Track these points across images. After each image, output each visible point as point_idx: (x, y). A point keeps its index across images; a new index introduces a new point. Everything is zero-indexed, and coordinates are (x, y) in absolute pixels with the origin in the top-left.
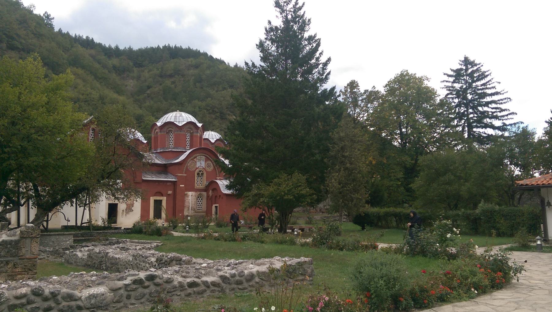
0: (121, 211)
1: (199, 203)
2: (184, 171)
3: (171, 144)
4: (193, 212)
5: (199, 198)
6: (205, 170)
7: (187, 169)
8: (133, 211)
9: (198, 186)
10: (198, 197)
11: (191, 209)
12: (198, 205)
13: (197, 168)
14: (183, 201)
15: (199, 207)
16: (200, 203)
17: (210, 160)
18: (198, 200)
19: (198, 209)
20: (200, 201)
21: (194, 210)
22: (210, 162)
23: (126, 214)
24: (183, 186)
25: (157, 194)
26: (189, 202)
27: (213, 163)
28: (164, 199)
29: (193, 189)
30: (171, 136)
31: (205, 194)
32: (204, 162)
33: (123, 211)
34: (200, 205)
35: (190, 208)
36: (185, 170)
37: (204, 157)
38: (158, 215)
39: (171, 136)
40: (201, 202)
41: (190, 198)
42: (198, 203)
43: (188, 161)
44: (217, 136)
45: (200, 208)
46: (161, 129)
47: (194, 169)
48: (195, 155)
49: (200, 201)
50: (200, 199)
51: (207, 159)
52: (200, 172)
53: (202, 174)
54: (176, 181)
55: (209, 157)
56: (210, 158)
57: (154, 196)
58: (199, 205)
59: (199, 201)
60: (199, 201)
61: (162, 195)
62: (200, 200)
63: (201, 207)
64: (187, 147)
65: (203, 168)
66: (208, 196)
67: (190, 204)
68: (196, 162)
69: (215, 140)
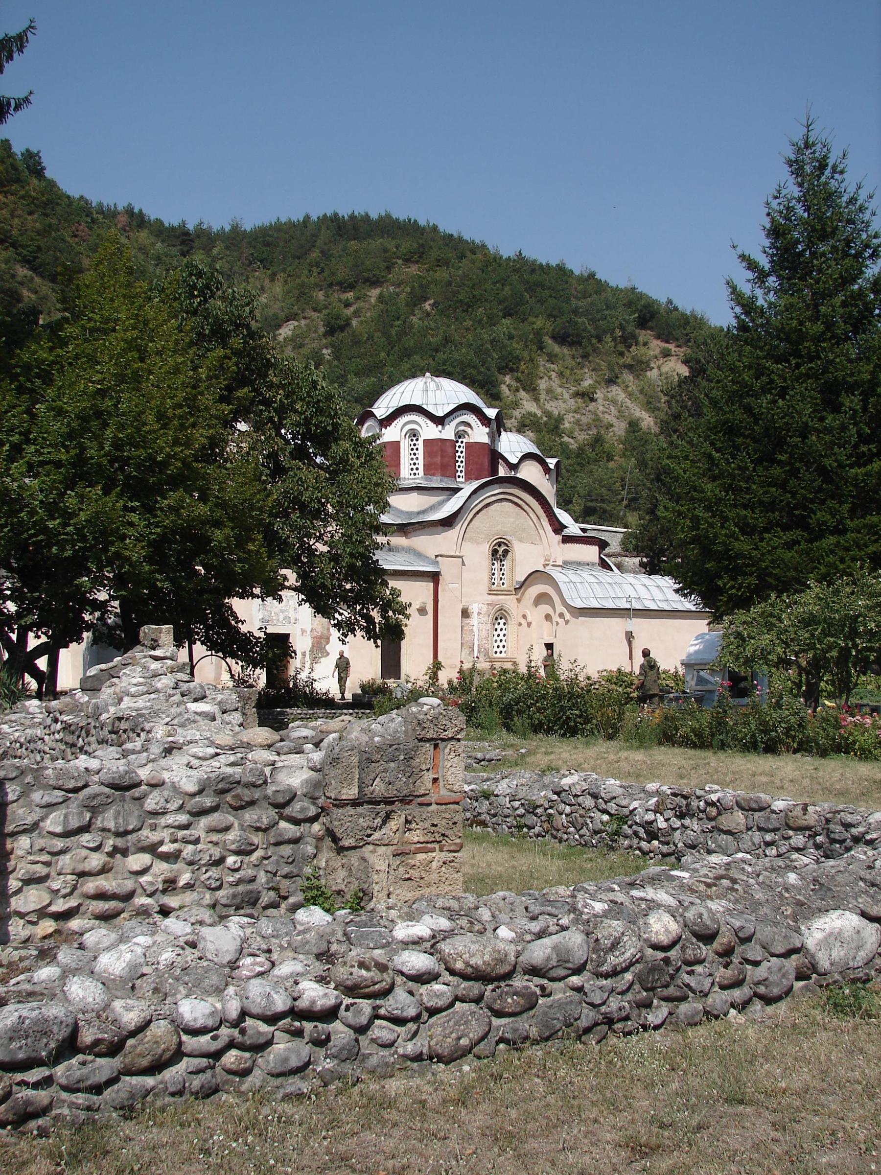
1: (499, 635)
10: (496, 619)
11: (479, 652)
12: (496, 641)
15: (498, 647)
16: (502, 633)
18: (496, 626)
19: (496, 652)
20: (501, 630)
33: (304, 654)
34: (501, 641)
44: (522, 444)
45: (501, 648)
49: (501, 630)
50: (502, 621)
52: (500, 546)
58: (499, 639)
59: (499, 628)
62: (502, 625)
63: (504, 647)
64: (459, 477)
69: (520, 455)
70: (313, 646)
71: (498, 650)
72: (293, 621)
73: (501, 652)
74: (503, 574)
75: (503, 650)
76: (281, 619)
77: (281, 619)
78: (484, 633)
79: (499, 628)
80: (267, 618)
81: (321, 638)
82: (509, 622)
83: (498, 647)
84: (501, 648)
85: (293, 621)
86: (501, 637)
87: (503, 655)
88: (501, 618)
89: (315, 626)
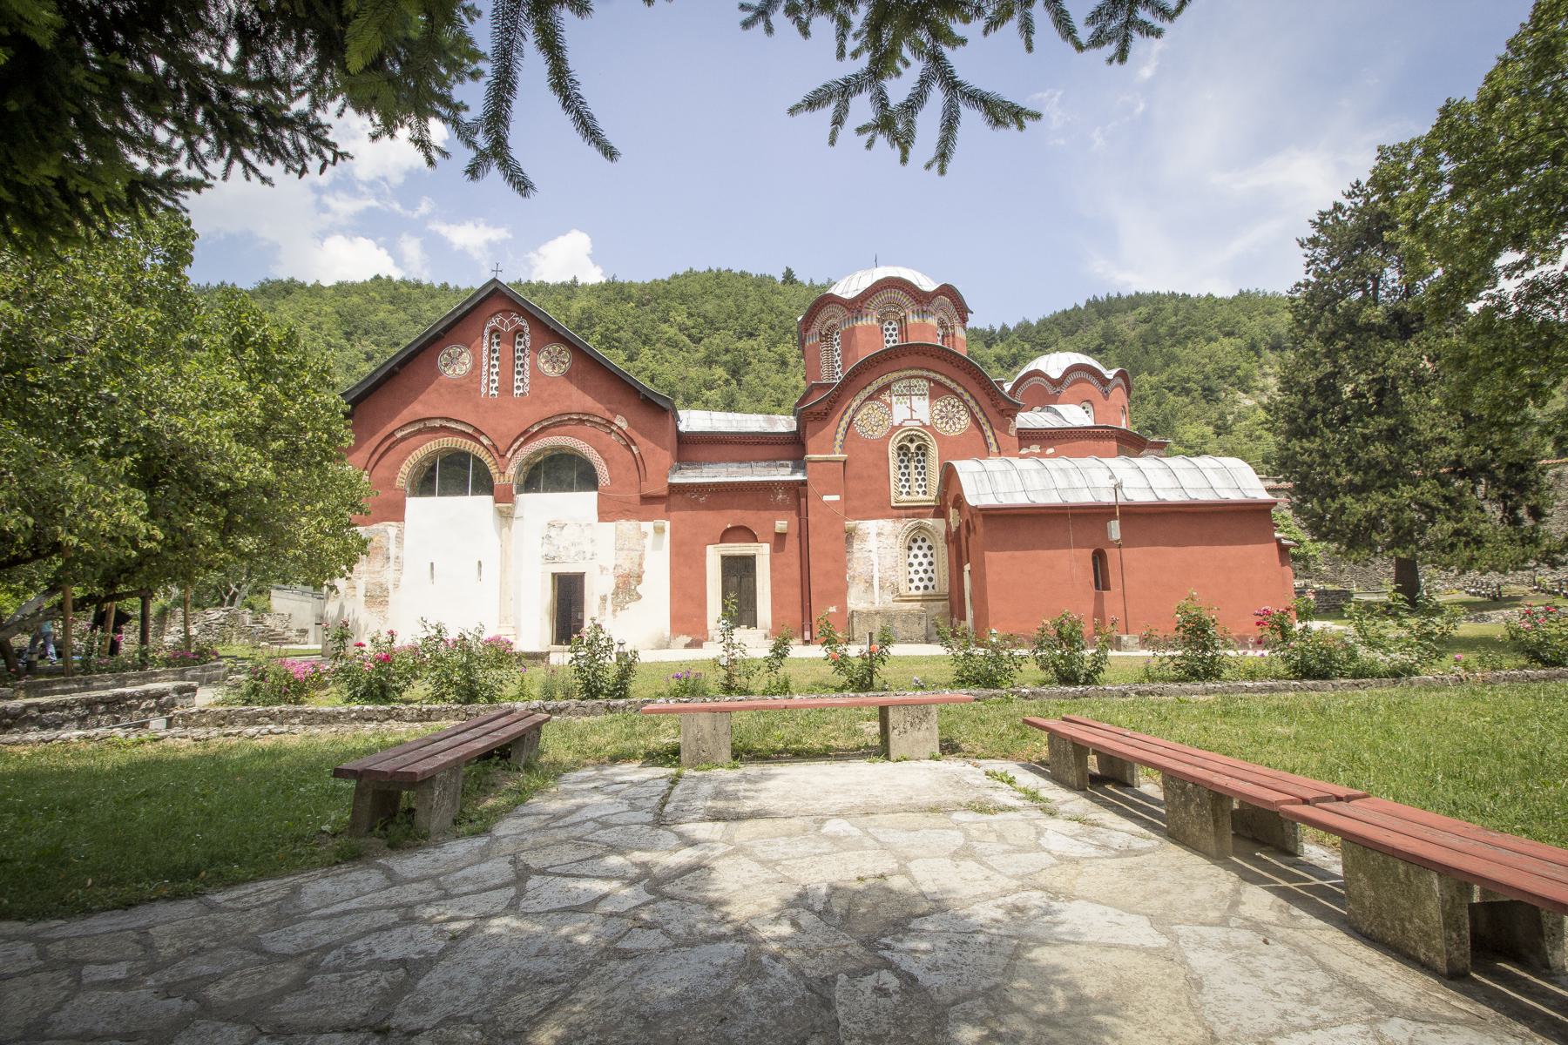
0: (599, 601)
1: (921, 564)
2: (838, 443)
4: (889, 598)
5: (920, 543)
6: (936, 434)
8: (640, 597)
9: (909, 498)
11: (881, 588)
13: (894, 429)
14: (841, 562)
17: (953, 392)
18: (915, 551)
22: (954, 401)
23: (614, 611)
24: (837, 498)
25: (727, 535)
27: (963, 401)
28: (762, 552)
29: (885, 509)
32: (927, 400)
33: (604, 599)
35: (876, 583)
38: (741, 610)
41: (872, 543)
42: (916, 562)
43: (854, 405)
47: (879, 433)
48: (880, 382)
50: (925, 545)
51: (938, 391)
52: (912, 441)
53: (922, 450)
54: (804, 483)
55: (948, 382)
56: (953, 385)
57: (722, 541)
61: (755, 539)
62: (925, 550)
65: (924, 426)
68: (890, 406)
70: (618, 587)
72: (588, 555)
75: (930, 585)
76: (573, 551)
78: (889, 562)
80: (553, 554)
81: (629, 576)
83: (921, 580)
84: (926, 582)
85: (588, 555)
87: (930, 591)
88: (924, 540)
89: (619, 563)
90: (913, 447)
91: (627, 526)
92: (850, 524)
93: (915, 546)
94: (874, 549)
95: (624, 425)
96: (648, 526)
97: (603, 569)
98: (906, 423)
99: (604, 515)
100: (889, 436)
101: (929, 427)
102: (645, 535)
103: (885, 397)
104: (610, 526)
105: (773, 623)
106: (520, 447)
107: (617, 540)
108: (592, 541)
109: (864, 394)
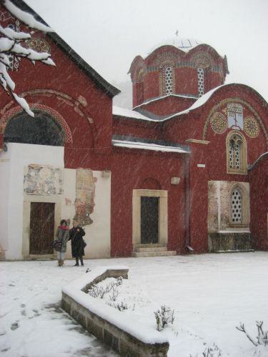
1: (235, 207)
3: (169, 90)
5: (235, 195)
6: (246, 137)
7: (210, 130)
8: (91, 222)
13: (229, 130)
15: (235, 215)
20: (237, 202)
21: (227, 221)
22: (253, 119)
24: (203, 166)
26: (216, 202)
27: (258, 121)
29: (223, 176)
30: (169, 75)
31: (246, 186)
36: (205, 130)
37: (241, 107)
39: (169, 75)
40: (239, 204)
41: (218, 194)
42: (233, 205)
43: (211, 112)
45: (237, 217)
46: (149, 64)
47: (221, 132)
48: (223, 102)
51: (247, 113)
52: (235, 138)
53: (240, 142)
57: (141, 188)
58: (235, 210)
60: (235, 201)
62: (237, 199)
65: (241, 130)
66: (252, 191)
67: (219, 208)
70: (77, 215)
71: (235, 218)
72: (58, 191)
73: (237, 220)
74: (238, 160)
75: (239, 218)
77: (46, 190)
79: (235, 201)
80: (32, 188)
81: (84, 207)
82: (244, 197)
84: (237, 217)
85: (58, 191)
86: (237, 208)
87: (239, 221)
88: (237, 194)
89: (79, 196)
90: (236, 141)
91: (83, 172)
92: (210, 182)
93: (233, 196)
94: (219, 197)
95: (85, 103)
96: (97, 174)
97: (68, 201)
98: (234, 128)
99: (72, 161)
100: (225, 135)
101: (243, 132)
102: (95, 180)
103: (224, 111)
104: (72, 172)
105: (169, 240)
106: (10, 108)
107: (77, 181)
108: (60, 181)
109: (215, 107)
